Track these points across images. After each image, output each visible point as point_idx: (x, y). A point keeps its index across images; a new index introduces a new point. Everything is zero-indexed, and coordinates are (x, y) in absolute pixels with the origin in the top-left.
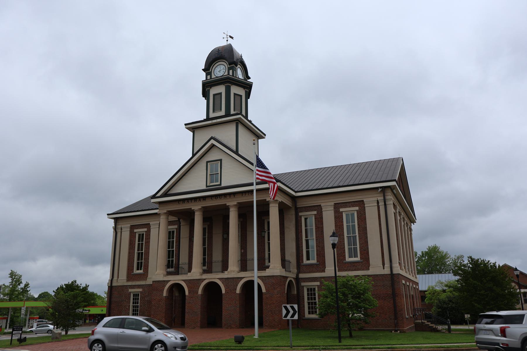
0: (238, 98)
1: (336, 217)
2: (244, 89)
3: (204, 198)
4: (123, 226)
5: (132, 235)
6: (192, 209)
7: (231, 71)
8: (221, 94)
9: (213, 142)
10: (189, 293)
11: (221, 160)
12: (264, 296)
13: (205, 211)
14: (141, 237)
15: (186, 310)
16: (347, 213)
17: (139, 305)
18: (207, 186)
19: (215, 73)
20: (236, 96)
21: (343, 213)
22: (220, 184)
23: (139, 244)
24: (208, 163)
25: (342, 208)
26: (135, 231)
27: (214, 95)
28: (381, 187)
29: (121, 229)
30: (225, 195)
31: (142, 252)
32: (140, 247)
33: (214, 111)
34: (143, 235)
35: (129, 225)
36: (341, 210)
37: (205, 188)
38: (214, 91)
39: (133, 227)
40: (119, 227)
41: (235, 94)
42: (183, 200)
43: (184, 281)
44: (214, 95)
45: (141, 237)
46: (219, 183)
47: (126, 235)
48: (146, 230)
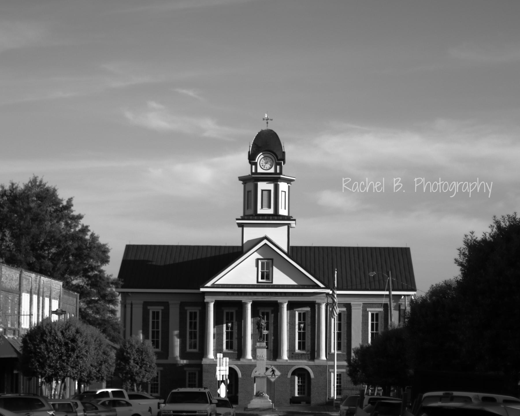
0: (283, 193)
1: (363, 316)
2: (288, 184)
3: (255, 294)
4: (133, 302)
5: (145, 313)
6: (243, 301)
7: (278, 167)
8: (269, 191)
9: (265, 241)
10: (242, 375)
11: (272, 259)
12: (312, 381)
13: (255, 305)
14: (156, 315)
15: (239, 390)
16: (373, 312)
17: (159, 382)
18: (258, 282)
19: (261, 165)
20: (282, 192)
21: (369, 312)
22: (272, 283)
23: (153, 322)
24: (259, 261)
25: (369, 308)
26: (149, 307)
27: (262, 191)
28: (403, 295)
29: (132, 304)
30: (276, 294)
31: (157, 330)
32: (155, 325)
33: (262, 207)
34: (158, 313)
35: (142, 302)
36: (368, 309)
37: (255, 283)
38: (262, 186)
39: (146, 304)
40: (128, 301)
41: (282, 191)
42: (233, 293)
43: (237, 365)
44: (262, 191)
45: (156, 315)
46: (271, 282)
47: (138, 312)
48: (162, 308)
